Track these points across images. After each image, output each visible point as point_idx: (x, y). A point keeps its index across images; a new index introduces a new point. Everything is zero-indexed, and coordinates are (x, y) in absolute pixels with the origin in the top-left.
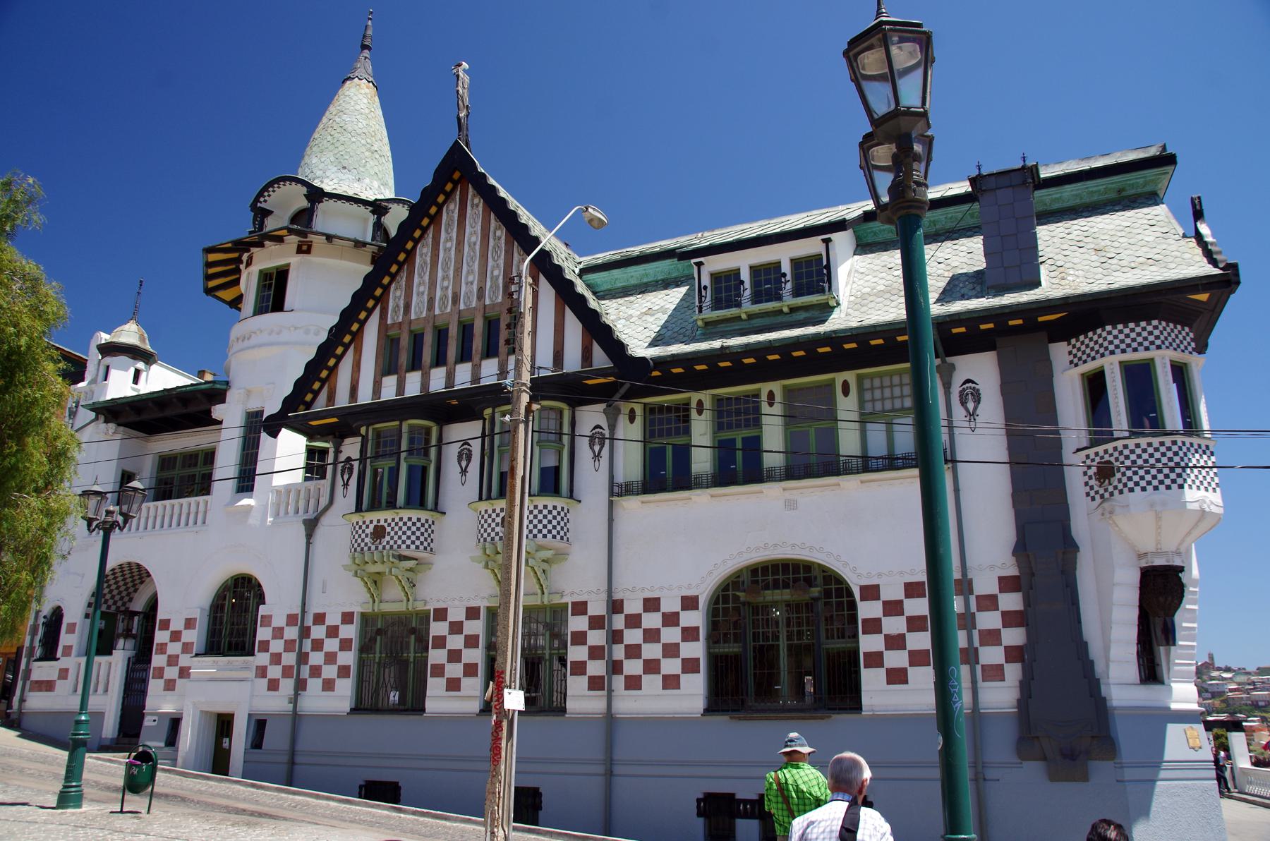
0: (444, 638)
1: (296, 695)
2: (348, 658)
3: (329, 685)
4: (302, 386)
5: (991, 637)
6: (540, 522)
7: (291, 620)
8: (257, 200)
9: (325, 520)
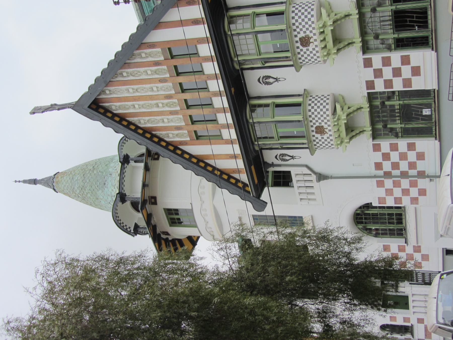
0: (385, 81)
1: (428, 176)
2: (402, 144)
3: (421, 156)
6: (303, 20)
7: (380, 184)
8: (129, 233)
9: (317, 169)
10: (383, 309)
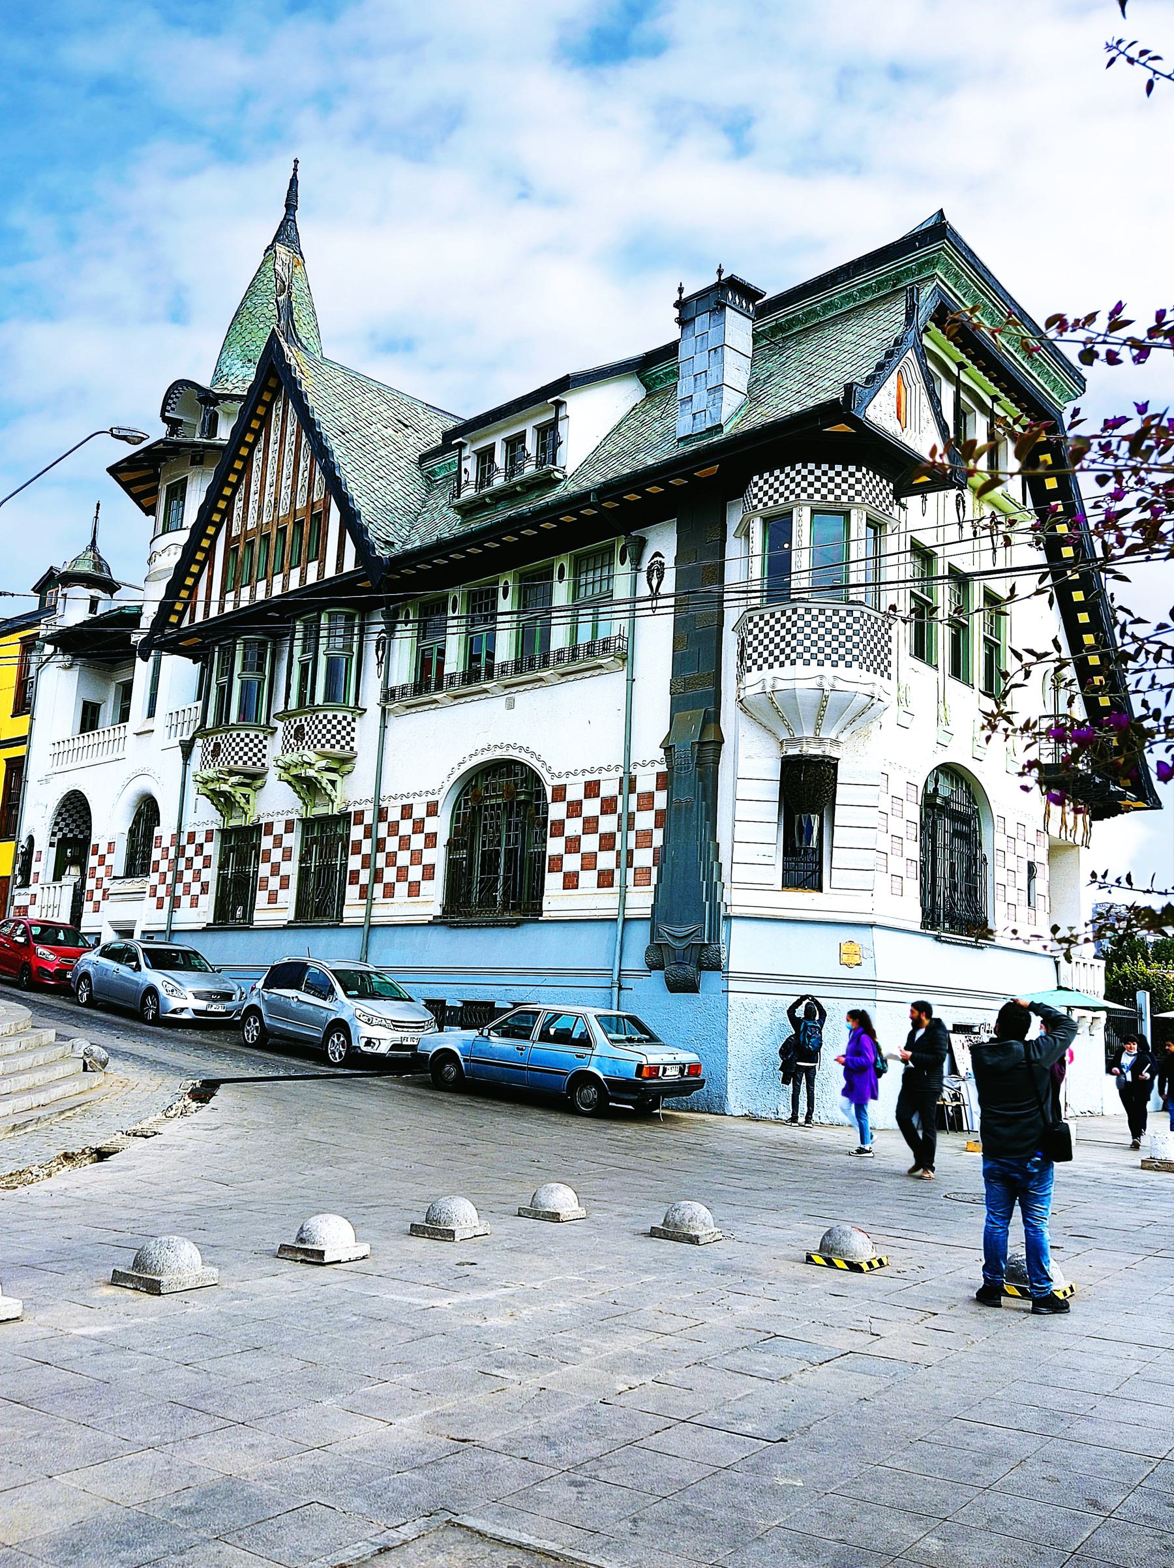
4: (165, 608)
5: (644, 839)
10: (55, 840)
